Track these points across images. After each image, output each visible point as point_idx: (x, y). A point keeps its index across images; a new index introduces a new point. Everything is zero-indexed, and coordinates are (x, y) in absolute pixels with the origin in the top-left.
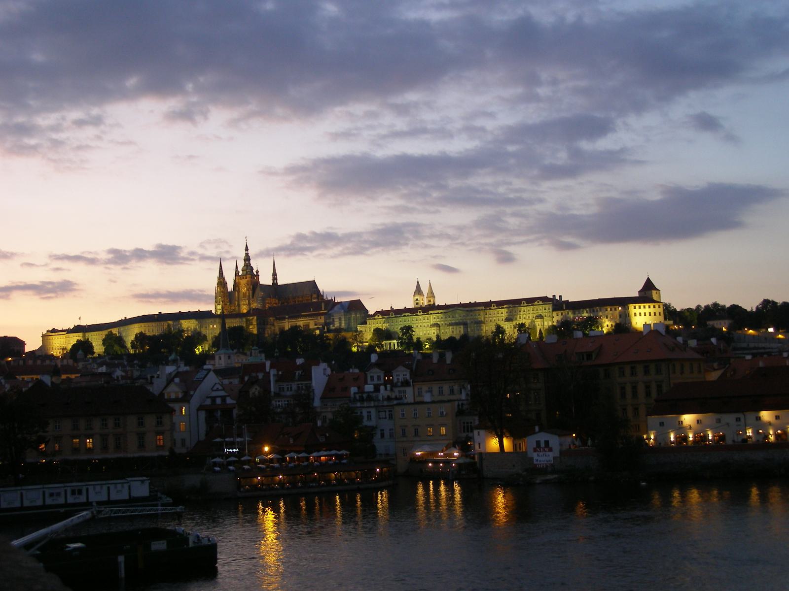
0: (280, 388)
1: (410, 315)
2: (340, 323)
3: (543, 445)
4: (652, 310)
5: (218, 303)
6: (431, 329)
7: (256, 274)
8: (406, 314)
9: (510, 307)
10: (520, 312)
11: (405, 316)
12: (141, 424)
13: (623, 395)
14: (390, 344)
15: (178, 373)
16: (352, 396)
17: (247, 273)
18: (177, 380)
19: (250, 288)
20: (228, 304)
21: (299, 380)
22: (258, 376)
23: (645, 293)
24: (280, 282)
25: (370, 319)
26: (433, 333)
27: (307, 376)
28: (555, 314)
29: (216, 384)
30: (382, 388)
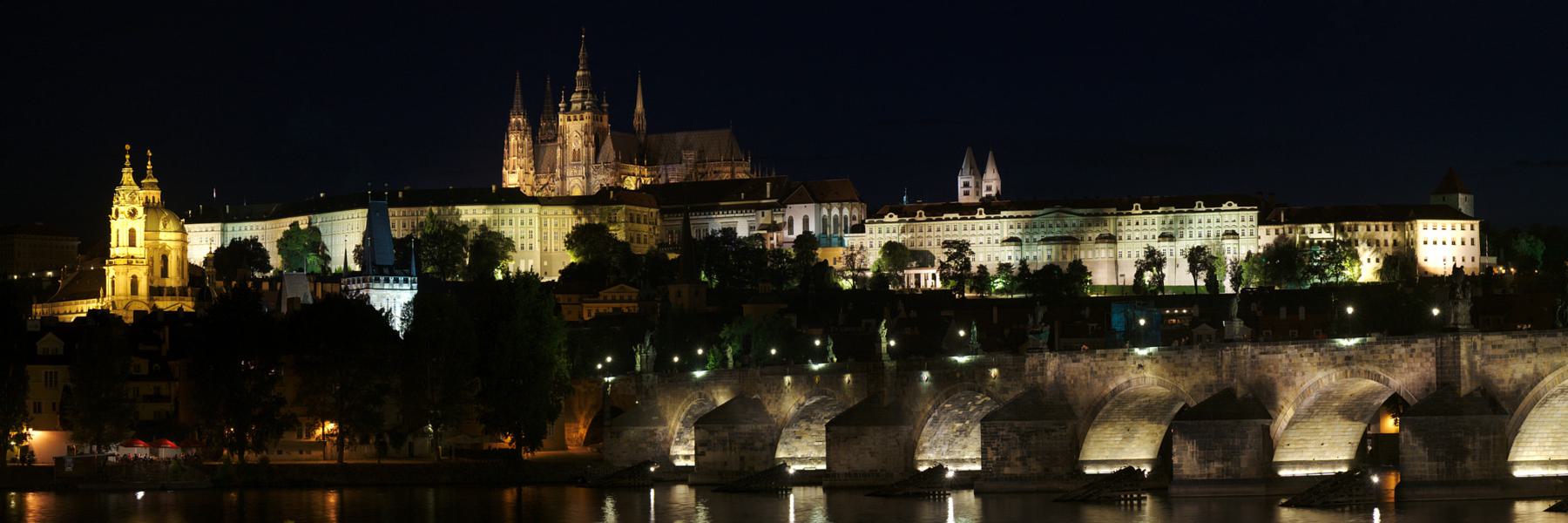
1: (959, 217)
4: (1458, 235)
5: (511, 169)
6: (1003, 248)
8: (951, 216)
9: (1171, 212)
10: (1191, 222)
11: (948, 219)
14: (918, 276)
17: (583, 108)
19: (589, 140)
20: (532, 172)
23: (1444, 199)
25: (873, 223)
26: (1010, 255)
28: (1263, 229)
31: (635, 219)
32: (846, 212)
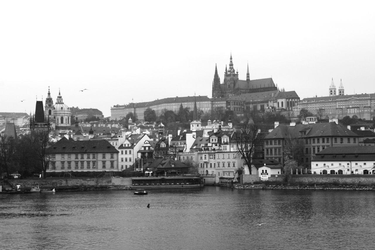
0: (173, 143)
2: (282, 106)
3: (265, 172)
7: (236, 73)
8: (322, 101)
12: (104, 157)
13: (314, 151)
15: (132, 135)
16: (201, 147)
18: (130, 139)
19: (232, 82)
21: (181, 140)
22: (165, 138)
24: (251, 79)
27: (184, 138)
29: (146, 141)
30: (214, 145)
31: (236, 104)
32: (293, 100)
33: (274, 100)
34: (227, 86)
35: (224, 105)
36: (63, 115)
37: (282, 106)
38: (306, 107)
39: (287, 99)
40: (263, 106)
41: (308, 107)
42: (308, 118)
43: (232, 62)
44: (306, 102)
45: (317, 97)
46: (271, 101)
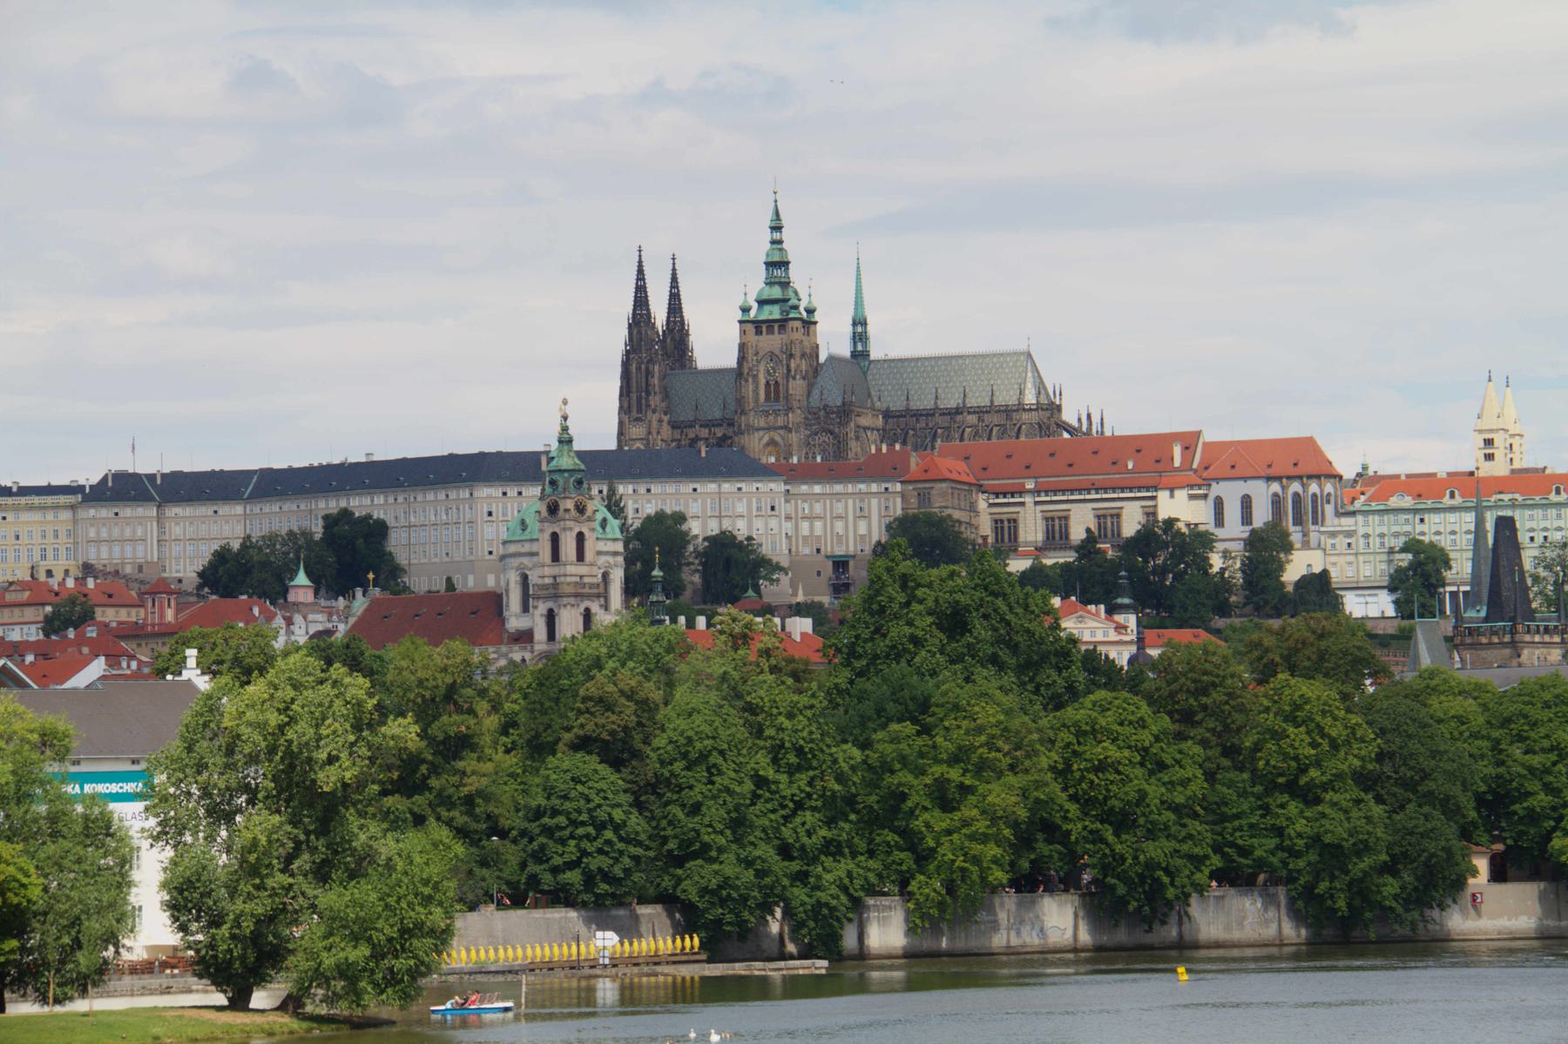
2: (1247, 517)
8: (1506, 497)
19: (798, 366)
32: (1314, 487)
33: (1191, 486)
34: (756, 391)
35: (850, 502)
36: (611, 559)
37: (1247, 517)
38: (1408, 528)
39: (1269, 479)
40: (1118, 516)
41: (1419, 528)
42: (1451, 593)
43: (785, 246)
44: (1408, 502)
45: (1371, 472)
46: (1172, 490)
